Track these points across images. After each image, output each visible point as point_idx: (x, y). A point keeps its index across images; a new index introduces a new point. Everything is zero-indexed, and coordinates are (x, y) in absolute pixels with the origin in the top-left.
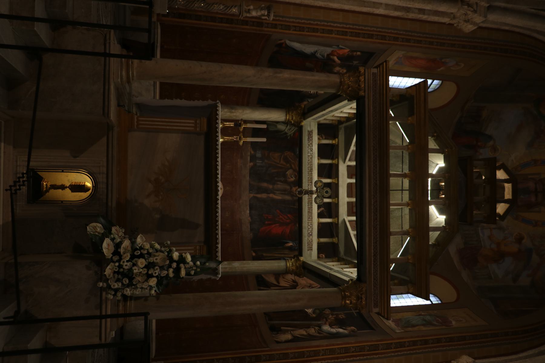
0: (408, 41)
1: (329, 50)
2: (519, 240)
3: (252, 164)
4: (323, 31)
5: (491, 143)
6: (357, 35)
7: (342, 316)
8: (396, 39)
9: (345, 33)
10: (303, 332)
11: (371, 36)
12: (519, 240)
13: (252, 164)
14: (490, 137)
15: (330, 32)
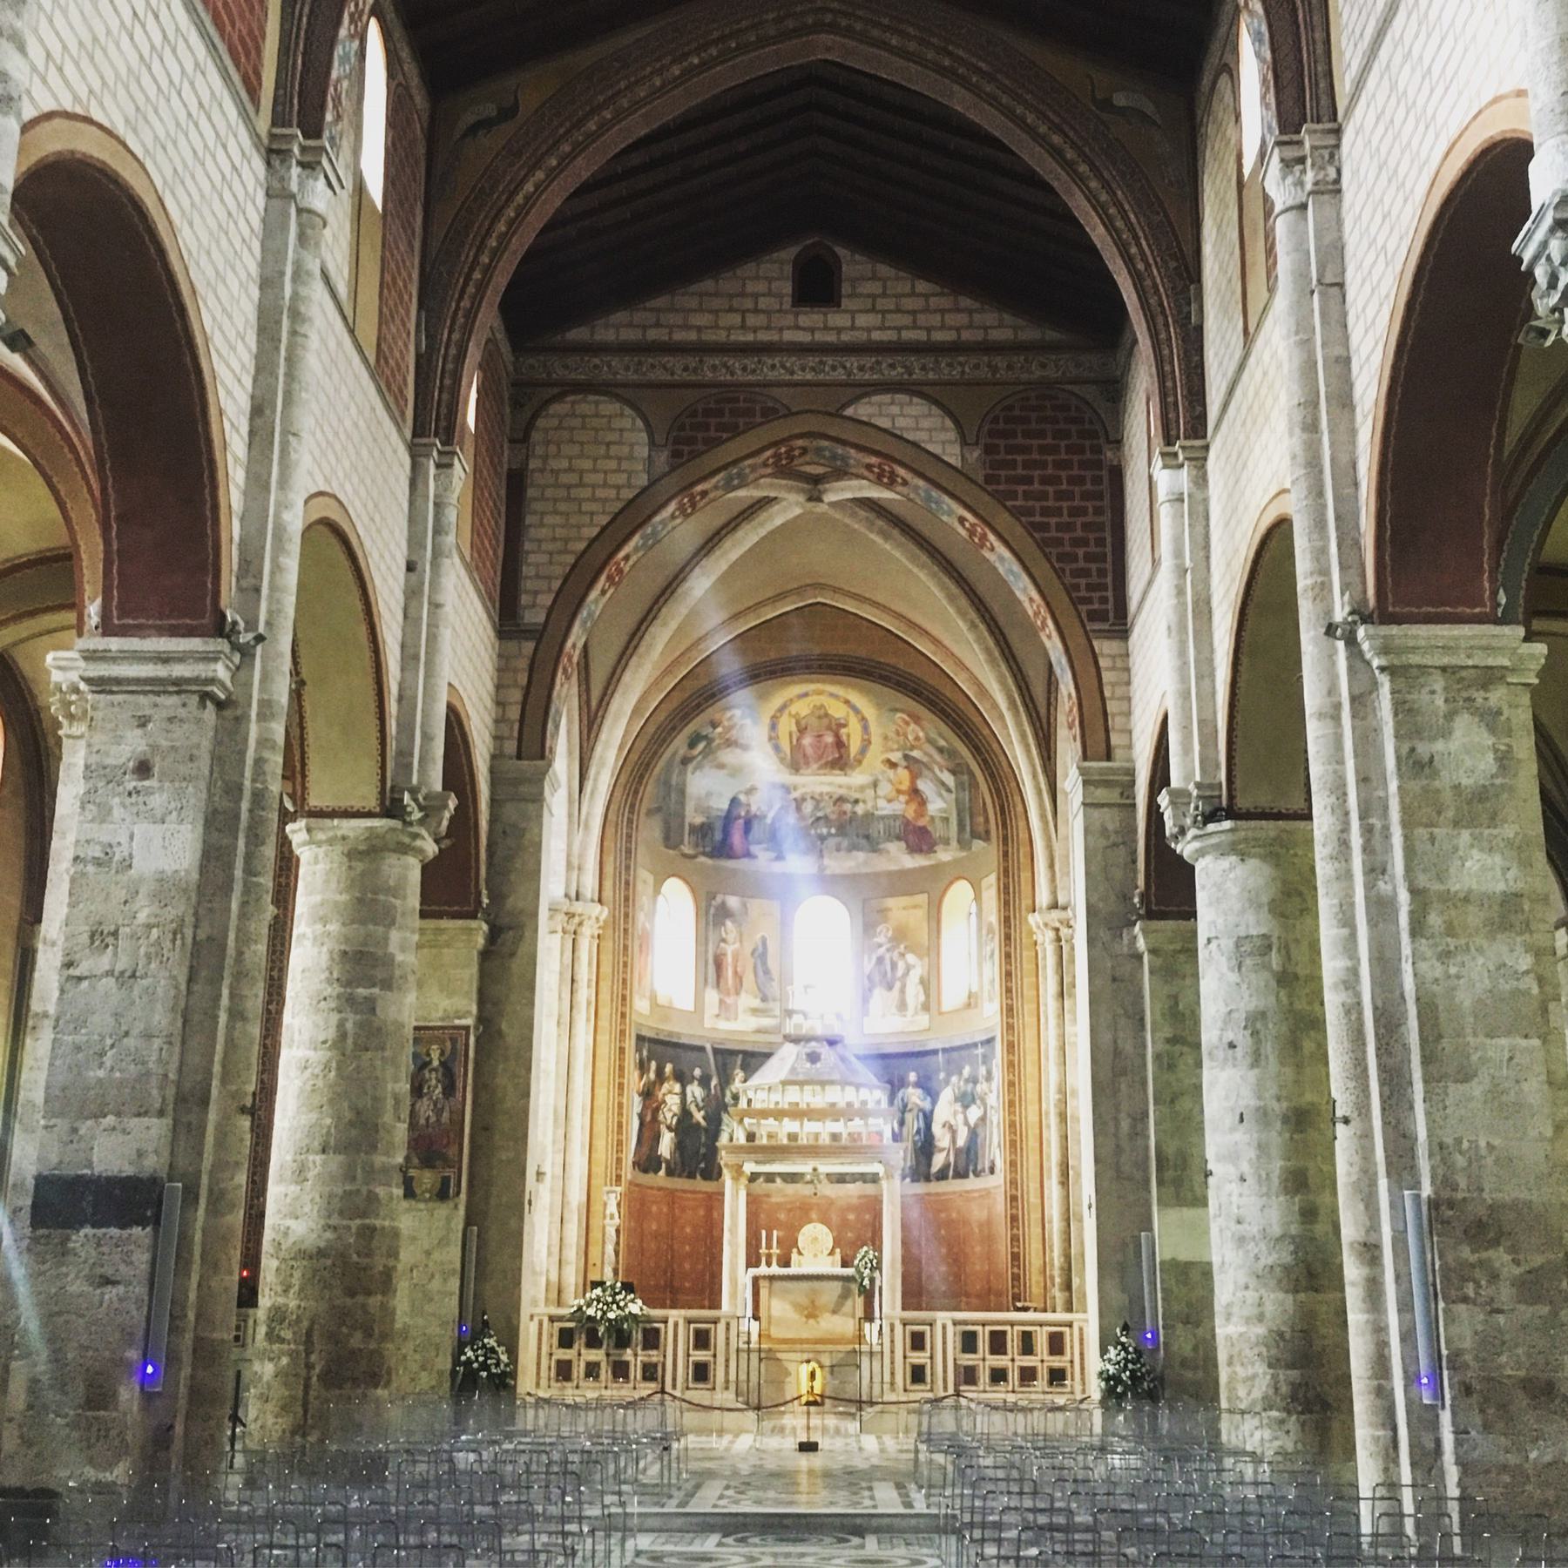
0: (624, 998)
1: (637, 1100)
2: (893, 765)
3: (778, 1180)
4: (620, 1114)
5: (742, 798)
6: (621, 1068)
7: (983, 1070)
8: (623, 1015)
9: (621, 1086)
10: (995, 1131)
11: (622, 1050)
12: (893, 765)
13: (778, 1180)
14: (734, 801)
15: (620, 1105)
